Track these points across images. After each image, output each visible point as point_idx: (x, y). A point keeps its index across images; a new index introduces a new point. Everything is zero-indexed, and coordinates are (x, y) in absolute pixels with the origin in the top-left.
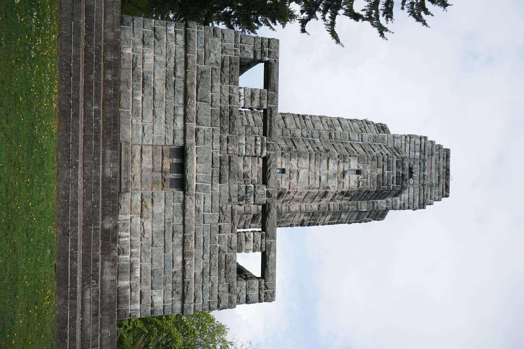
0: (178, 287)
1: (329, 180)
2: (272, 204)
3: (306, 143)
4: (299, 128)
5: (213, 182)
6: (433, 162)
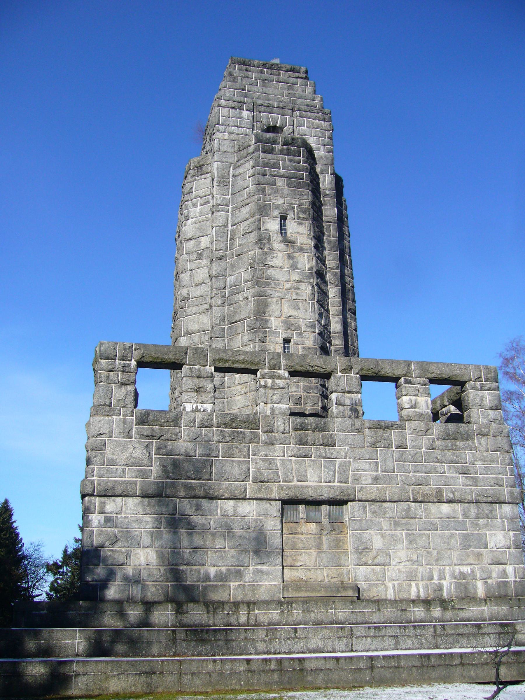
0: (483, 510)
5: (333, 456)
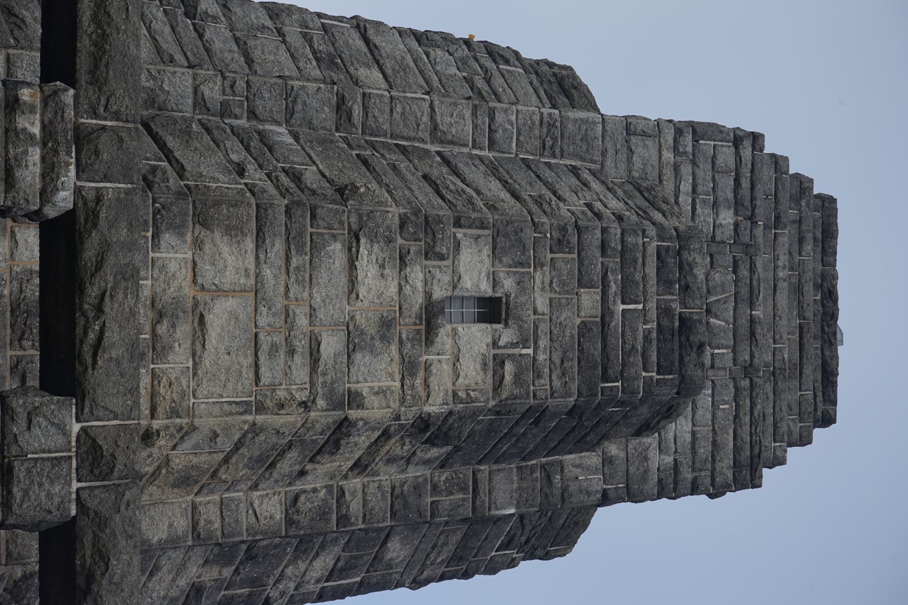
1: (358, 357)
2: (117, 518)
3: (228, 144)
4: (172, 60)
6: (781, 257)
